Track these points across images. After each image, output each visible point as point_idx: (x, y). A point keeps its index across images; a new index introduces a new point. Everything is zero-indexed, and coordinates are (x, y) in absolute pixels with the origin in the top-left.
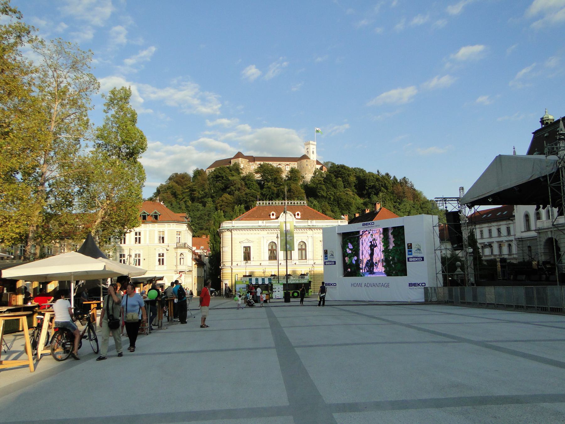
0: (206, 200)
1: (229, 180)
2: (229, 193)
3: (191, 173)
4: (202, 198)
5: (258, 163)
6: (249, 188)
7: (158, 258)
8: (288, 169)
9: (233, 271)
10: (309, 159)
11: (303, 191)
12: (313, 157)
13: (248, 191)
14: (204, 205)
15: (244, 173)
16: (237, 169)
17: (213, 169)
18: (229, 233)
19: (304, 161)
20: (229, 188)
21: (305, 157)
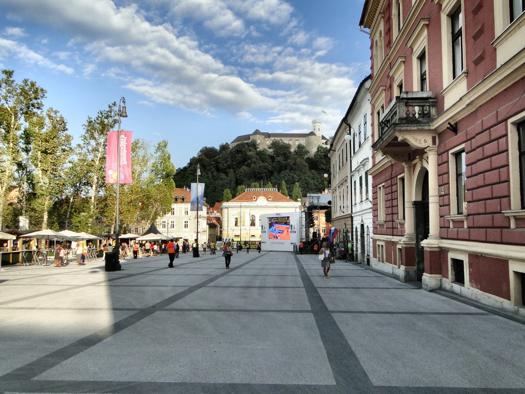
0: (228, 170)
1: (247, 155)
2: (247, 166)
3: (218, 148)
4: (225, 169)
5: (273, 139)
6: (263, 161)
7: (184, 224)
8: (297, 143)
9: (229, 232)
10: (315, 135)
11: (307, 164)
12: (319, 134)
13: (261, 164)
14: (227, 176)
15: (261, 148)
16: (254, 145)
17: (236, 144)
18: (226, 209)
19: (313, 137)
20: (246, 161)
21: (312, 134)
